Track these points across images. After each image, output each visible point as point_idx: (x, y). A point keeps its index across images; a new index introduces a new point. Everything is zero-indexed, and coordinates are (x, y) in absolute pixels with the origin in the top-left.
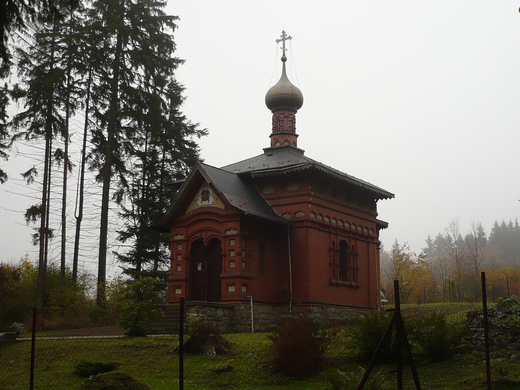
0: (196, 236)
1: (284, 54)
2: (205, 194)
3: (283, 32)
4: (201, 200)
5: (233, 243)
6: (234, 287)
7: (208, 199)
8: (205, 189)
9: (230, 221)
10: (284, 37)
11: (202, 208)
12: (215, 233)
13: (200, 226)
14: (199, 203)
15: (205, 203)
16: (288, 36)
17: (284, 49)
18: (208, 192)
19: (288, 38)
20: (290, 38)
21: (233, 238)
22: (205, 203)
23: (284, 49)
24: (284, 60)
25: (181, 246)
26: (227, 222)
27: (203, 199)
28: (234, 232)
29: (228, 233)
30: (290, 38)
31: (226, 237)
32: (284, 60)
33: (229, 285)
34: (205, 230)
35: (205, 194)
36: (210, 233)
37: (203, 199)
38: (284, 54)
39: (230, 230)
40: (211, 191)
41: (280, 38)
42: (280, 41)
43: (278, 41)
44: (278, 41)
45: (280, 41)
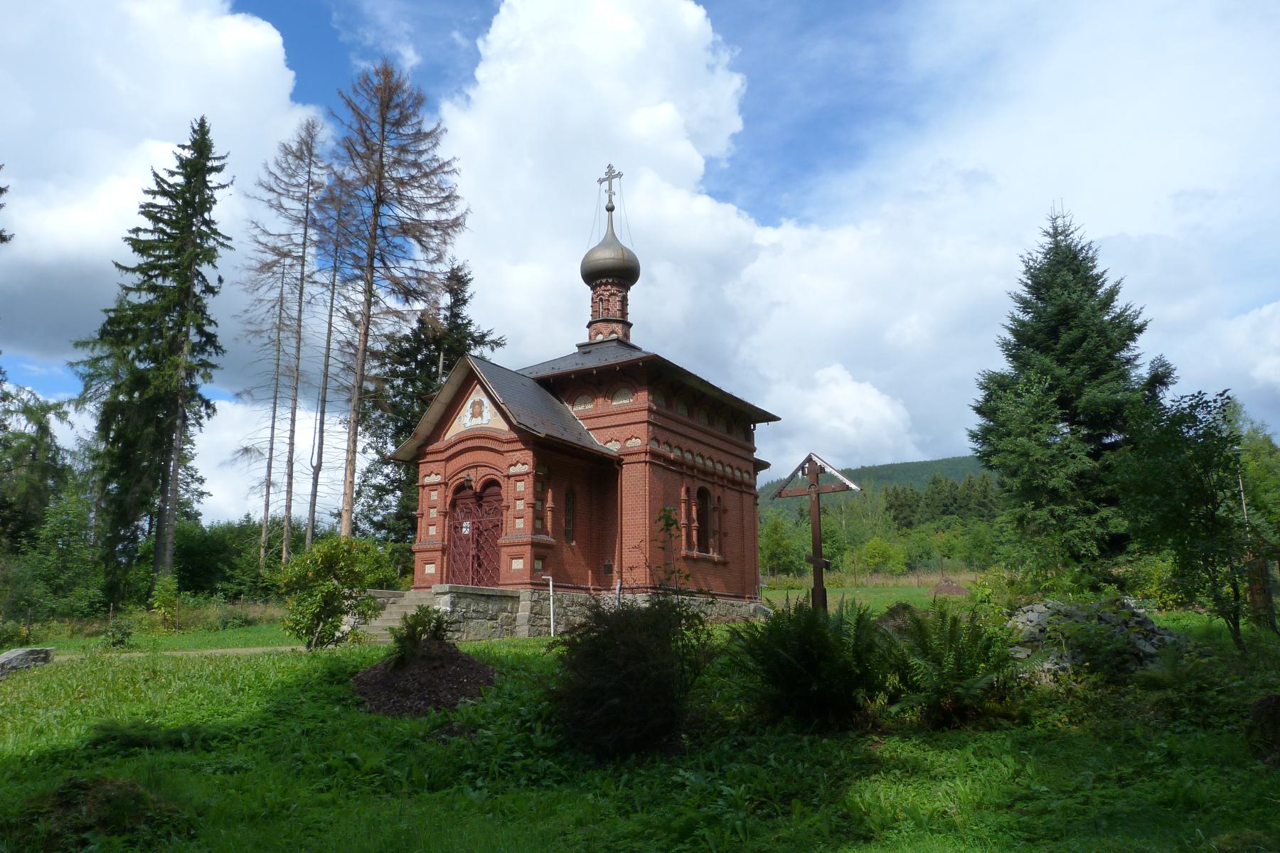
1: (610, 201)
5: (521, 486)
7: (480, 414)
8: (477, 399)
10: (611, 175)
12: (491, 471)
15: (477, 422)
17: (610, 193)
18: (481, 403)
20: (620, 175)
27: (473, 415)
28: (525, 469)
29: (513, 470)
30: (620, 175)
31: (509, 477)
32: (610, 209)
36: (482, 471)
37: (473, 415)
38: (610, 201)
42: (604, 180)
43: (601, 181)
44: (601, 181)
45: (604, 180)
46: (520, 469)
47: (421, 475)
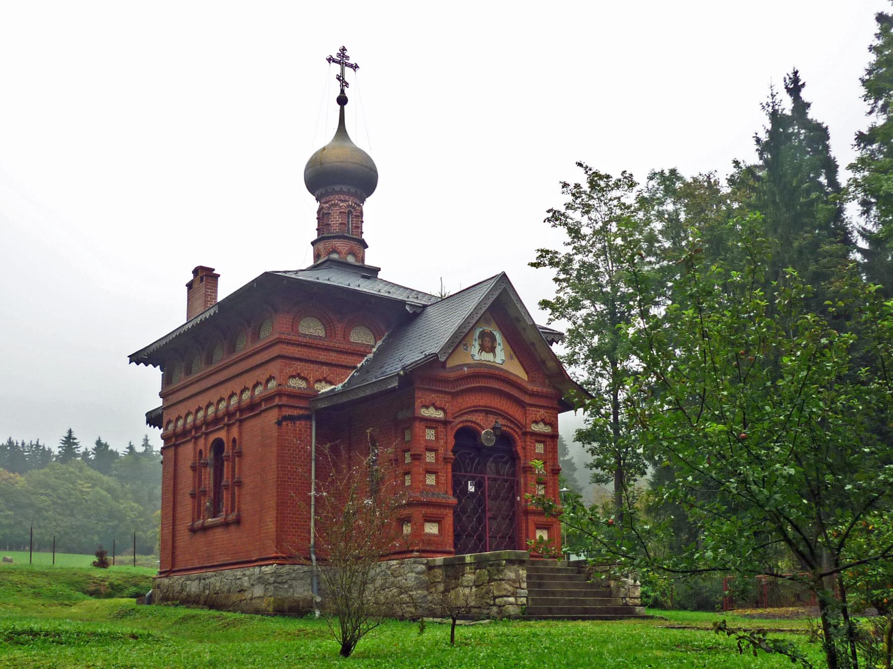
0: (464, 418)
1: (342, 91)
2: (487, 339)
4: (478, 347)
7: (492, 350)
8: (488, 329)
9: (540, 407)
10: (342, 59)
11: (481, 365)
12: (504, 422)
14: (475, 354)
15: (487, 357)
18: (493, 339)
19: (351, 66)
20: (355, 67)
21: (543, 439)
22: (487, 357)
23: (341, 78)
24: (342, 100)
25: (433, 432)
27: (483, 348)
30: (355, 67)
31: (534, 434)
32: (342, 100)
33: (540, 527)
34: (488, 411)
37: (483, 348)
38: (342, 91)
41: (335, 57)
42: (334, 61)
43: (330, 60)
44: (330, 60)
47: (418, 403)
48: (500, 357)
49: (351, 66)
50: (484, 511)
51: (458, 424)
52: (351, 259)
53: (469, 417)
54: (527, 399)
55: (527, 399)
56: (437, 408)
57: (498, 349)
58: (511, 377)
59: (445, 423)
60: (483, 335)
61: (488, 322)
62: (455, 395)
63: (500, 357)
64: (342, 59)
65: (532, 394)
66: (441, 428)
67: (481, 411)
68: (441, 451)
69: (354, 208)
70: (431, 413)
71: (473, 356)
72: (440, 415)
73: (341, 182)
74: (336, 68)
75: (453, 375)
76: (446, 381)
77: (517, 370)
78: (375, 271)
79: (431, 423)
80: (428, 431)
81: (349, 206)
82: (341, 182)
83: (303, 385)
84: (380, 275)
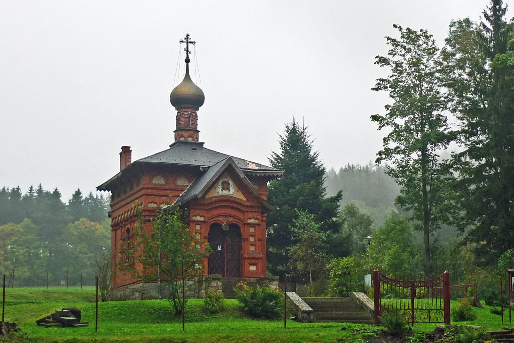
1: (188, 56)
2: (226, 184)
3: (188, 35)
4: (221, 188)
6: (255, 266)
7: (228, 189)
8: (226, 180)
9: (252, 212)
10: (187, 40)
11: (222, 196)
12: (234, 219)
13: (222, 211)
14: (220, 191)
15: (225, 192)
16: (192, 40)
17: (187, 50)
18: (228, 184)
19: (192, 43)
20: (194, 43)
22: (225, 192)
23: (187, 50)
24: (187, 61)
25: (199, 226)
26: (250, 212)
27: (223, 189)
29: (249, 221)
32: (187, 61)
35: (226, 184)
37: (223, 189)
38: (188, 56)
39: (250, 219)
40: (231, 183)
41: (184, 40)
42: (183, 42)
43: (181, 42)
44: (181, 42)
46: (253, 221)
48: (232, 191)
49: (192, 43)
50: (224, 258)
51: (211, 222)
52: (190, 140)
53: (217, 219)
54: (245, 209)
55: (245, 209)
56: (201, 216)
57: (231, 188)
58: (236, 200)
59: (204, 222)
60: (223, 183)
61: (226, 177)
62: (209, 210)
63: (232, 191)
64: (187, 40)
65: (248, 207)
66: (203, 224)
67: (222, 216)
68: (203, 234)
69: (192, 114)
70: (198, 218)
71: (218, 193)
72: (202, 219)
73: (187, 102)
74: (184, 45)
75: (207, 202)
76: (205, 205)
77: (241, 196)
78: (202, 144)
79: (198, 222)
80: (197, 226)
81: (189, 114)
82: (187, 102)
83: (155, 205)
84: (204, 146)
